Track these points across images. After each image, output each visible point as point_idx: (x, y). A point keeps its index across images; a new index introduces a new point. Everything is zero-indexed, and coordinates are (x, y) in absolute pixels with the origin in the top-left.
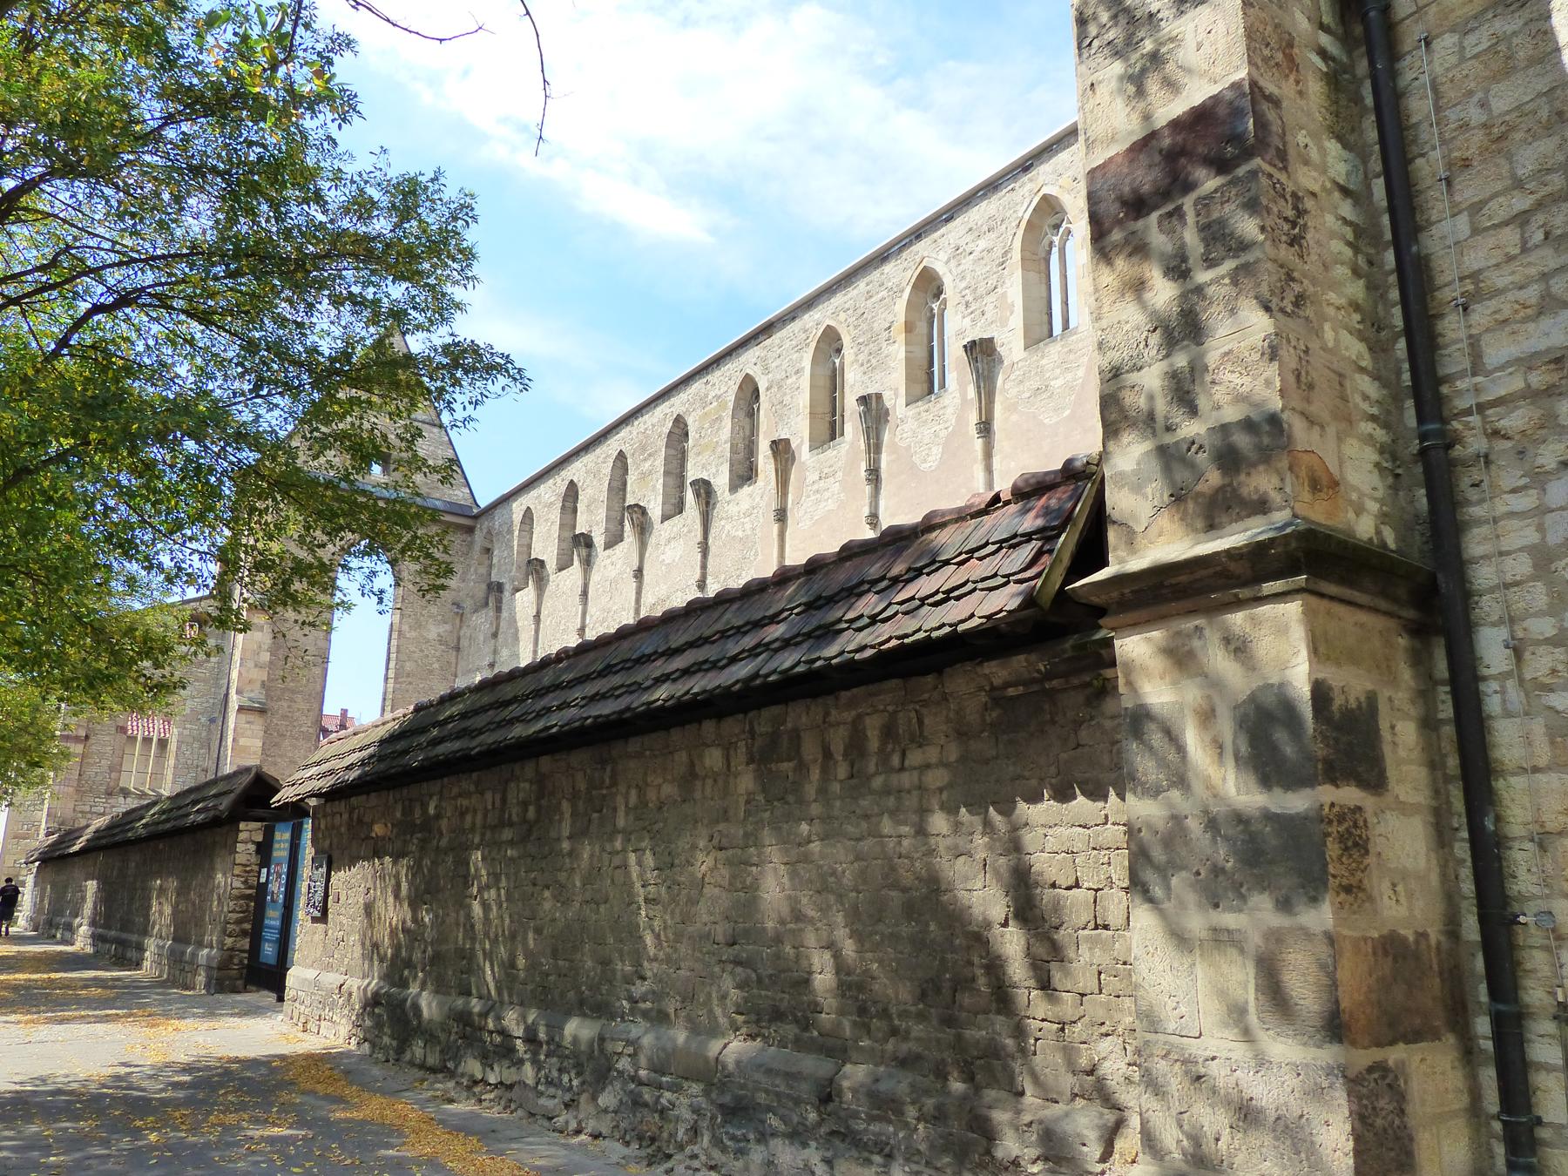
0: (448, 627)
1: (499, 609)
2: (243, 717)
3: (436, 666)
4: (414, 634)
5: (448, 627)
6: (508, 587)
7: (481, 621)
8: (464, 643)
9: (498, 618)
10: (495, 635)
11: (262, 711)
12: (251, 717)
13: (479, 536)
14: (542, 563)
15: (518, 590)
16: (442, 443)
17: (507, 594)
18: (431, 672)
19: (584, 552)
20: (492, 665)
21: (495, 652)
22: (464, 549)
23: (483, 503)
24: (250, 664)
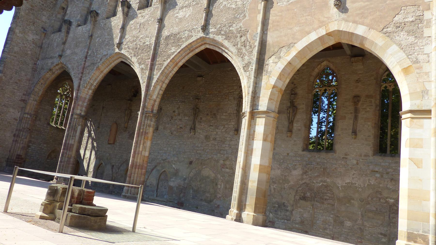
0: (37, 37)
1: (68, 33)
4: (21, 35)
6: (74, 24)
9: (67, 36)
10: (64, 43)
14: (97, 14)
17: (73, 27)
18: (27, 54)
20: (60, 56)
21: (63, 51)
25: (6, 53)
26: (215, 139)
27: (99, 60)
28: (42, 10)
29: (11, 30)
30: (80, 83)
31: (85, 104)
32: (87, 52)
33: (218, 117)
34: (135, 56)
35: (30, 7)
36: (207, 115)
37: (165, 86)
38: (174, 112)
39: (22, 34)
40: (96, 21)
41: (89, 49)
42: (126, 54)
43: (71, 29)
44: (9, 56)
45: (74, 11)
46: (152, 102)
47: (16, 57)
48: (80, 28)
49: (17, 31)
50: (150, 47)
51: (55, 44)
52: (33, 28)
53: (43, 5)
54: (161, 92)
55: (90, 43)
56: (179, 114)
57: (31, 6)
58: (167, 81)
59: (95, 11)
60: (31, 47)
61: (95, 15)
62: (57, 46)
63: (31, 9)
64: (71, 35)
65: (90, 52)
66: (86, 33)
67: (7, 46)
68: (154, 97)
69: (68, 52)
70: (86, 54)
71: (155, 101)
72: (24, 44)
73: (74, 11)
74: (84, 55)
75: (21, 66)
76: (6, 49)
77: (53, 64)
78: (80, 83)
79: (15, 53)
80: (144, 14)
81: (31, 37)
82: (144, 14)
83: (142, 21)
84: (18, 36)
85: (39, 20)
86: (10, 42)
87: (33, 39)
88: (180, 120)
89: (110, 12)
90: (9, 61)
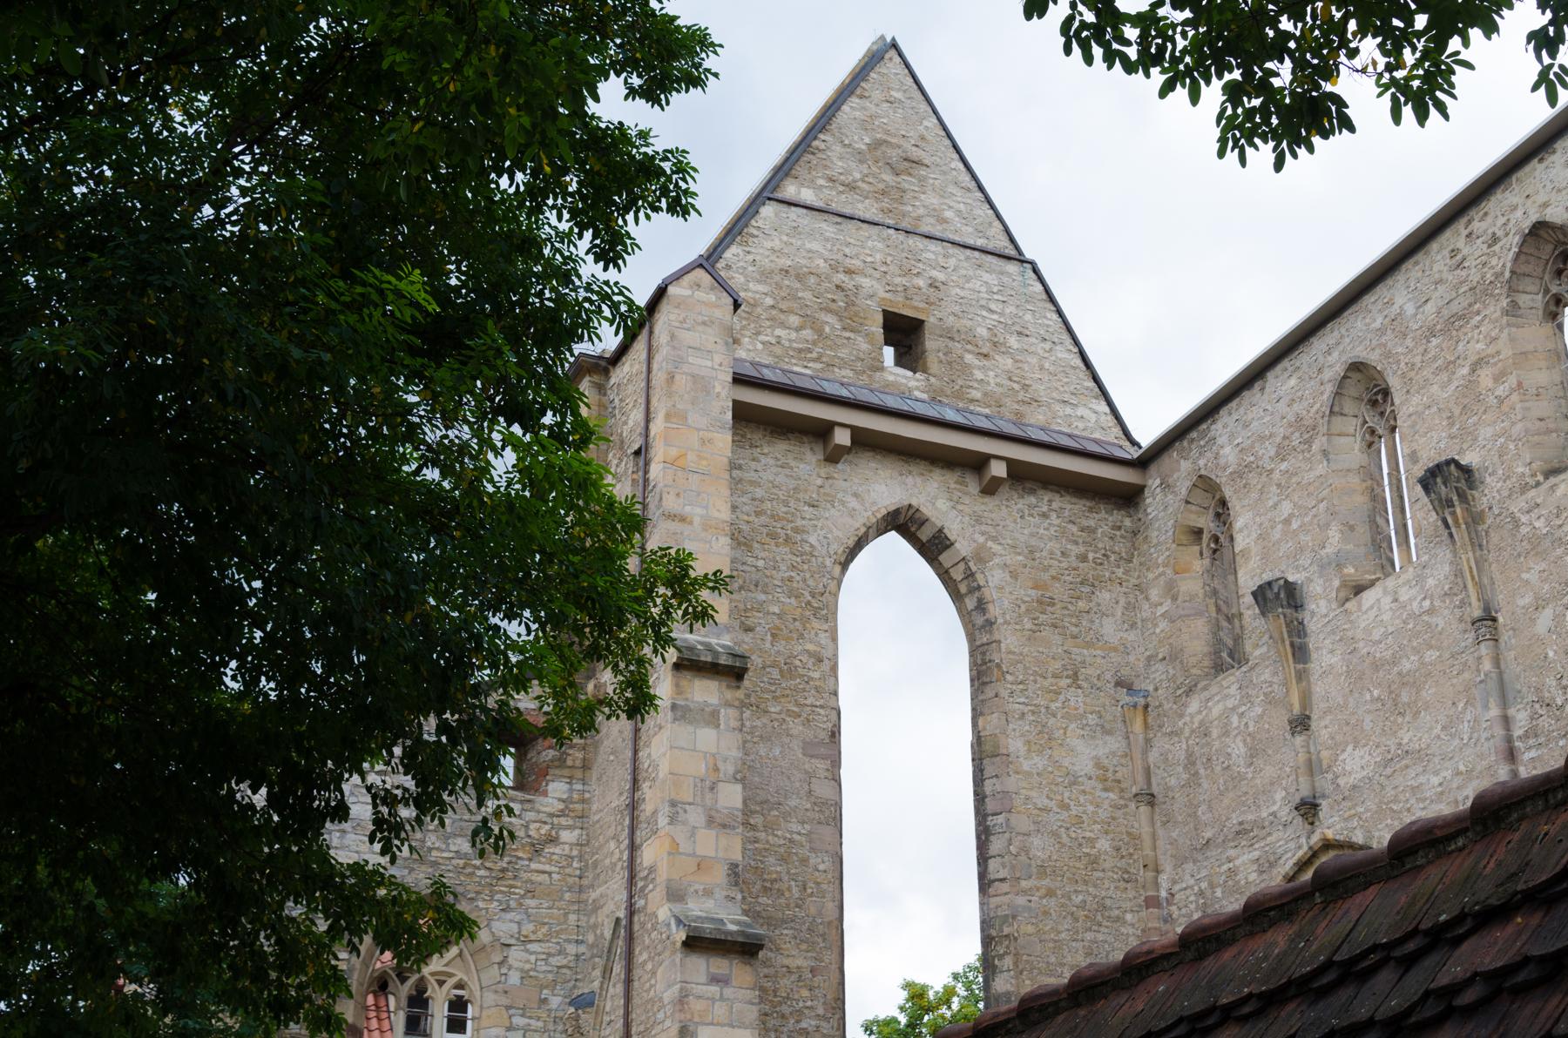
0: (1115, 743)
1: (1300, 653)
2: (700, 966)
3: (1104, 844)
4: (1039, 762)
5: (1115, 743)
7: (1235, 709)
8: (1169, 779)
9: (1301, 676)
11: (746, 949)
12: (720, 965)
13: (1165, 504)
15: (1359, 589)
16: (1030, 299)
17: (1319, 607)
20: (1308, 809)
22: (1121, 547)
23: (1147, 432)
24: (695, 817)
25: (1005, 887)
28: (1086, 589)
29: (984, 754)
32: (1506, 721)
35: (1033, 593)
39: (1040, 753)
40: (1475, 519)
41: (1504, 702)
43: (1312, 625)
44: (1021, 901)
45: (1287, 521)
47: (1050, 893)
48: (1369, 597)
49: (1015, 745)
51: (1238, 749)
52: (1076, 699)
53: (1084, 558)
55: (1497, 661)
57: (1035, 587)
59: (1453, 460)
60: (1103, 814)
61: (1463, 485)
62: (1253, 754)
63: (1040, 602)
64: (1326, 657)
65: (1521, 718)
66: (1431, 611)
67: (996, 845)
69: (1355, 764)
70: (1499, 731)
72: (1066, 807)
73: (1287, 521)
74: (1498, 741)
75: (1089, 936)
76: (993, 865)
77: (1272, 865)
79: (1042, 871)
81: (1084, 753)
84: (1029, 774)
85: (1089, 645)
86: (1000, 819)
87: (1098, 765)
89: (1549, 431)
90: (1030, 929)
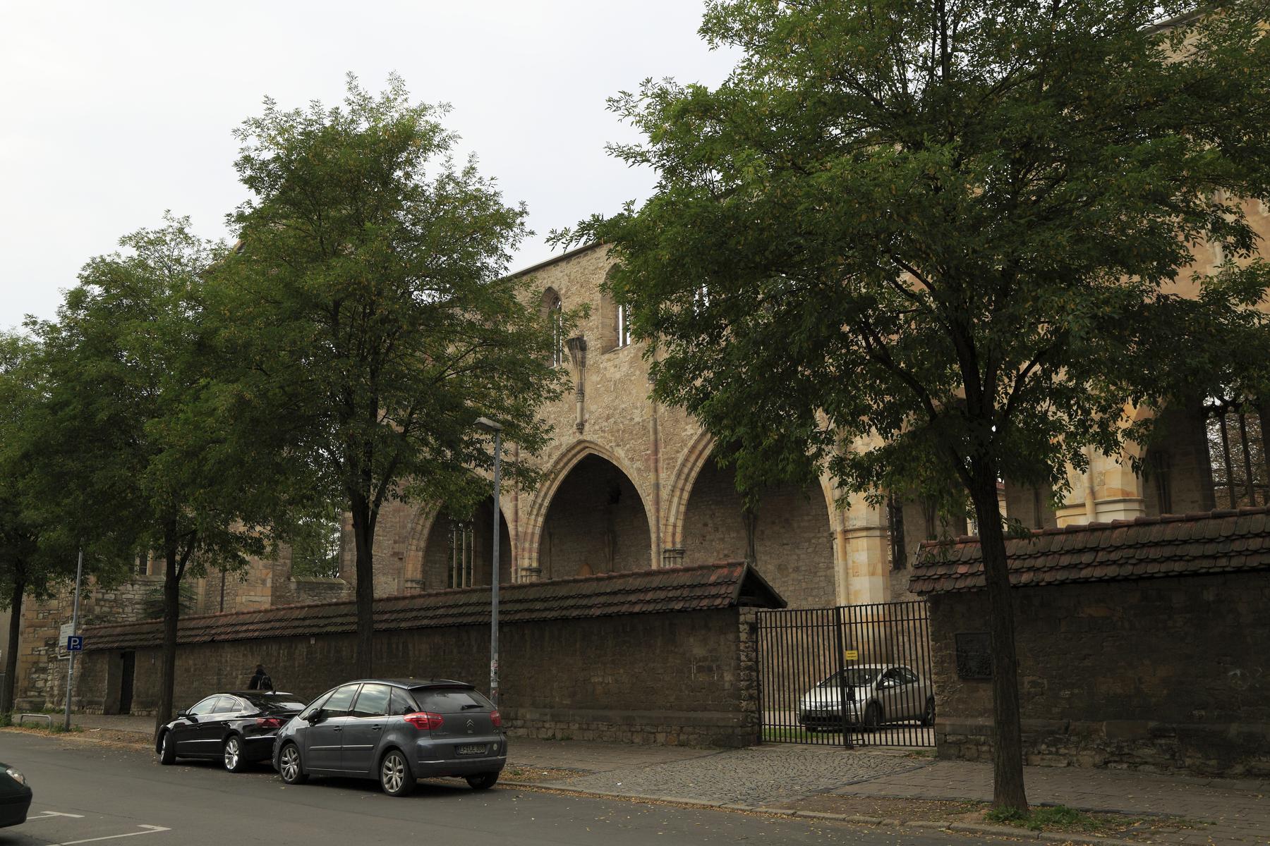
19: (579, 354)
26: (797, 569)
27: (545, 458)
30: (516, 506)
31: (536, 545)
33: (795, 525)
34: (618, 445)
36: (773, 523)
37: (686, 495)
38: (706, 525)
42: (600, 441)
46: (670, 529)
50: (644, 428)
54: (682, 509)
56: (717, 530)
58: (689, 487)
68: (672, 520)
71: (675, 526)
78: (516, 506)
80: (617, 362)
82: (617, 362)
83: (618, 376)
88: (722, 540)
